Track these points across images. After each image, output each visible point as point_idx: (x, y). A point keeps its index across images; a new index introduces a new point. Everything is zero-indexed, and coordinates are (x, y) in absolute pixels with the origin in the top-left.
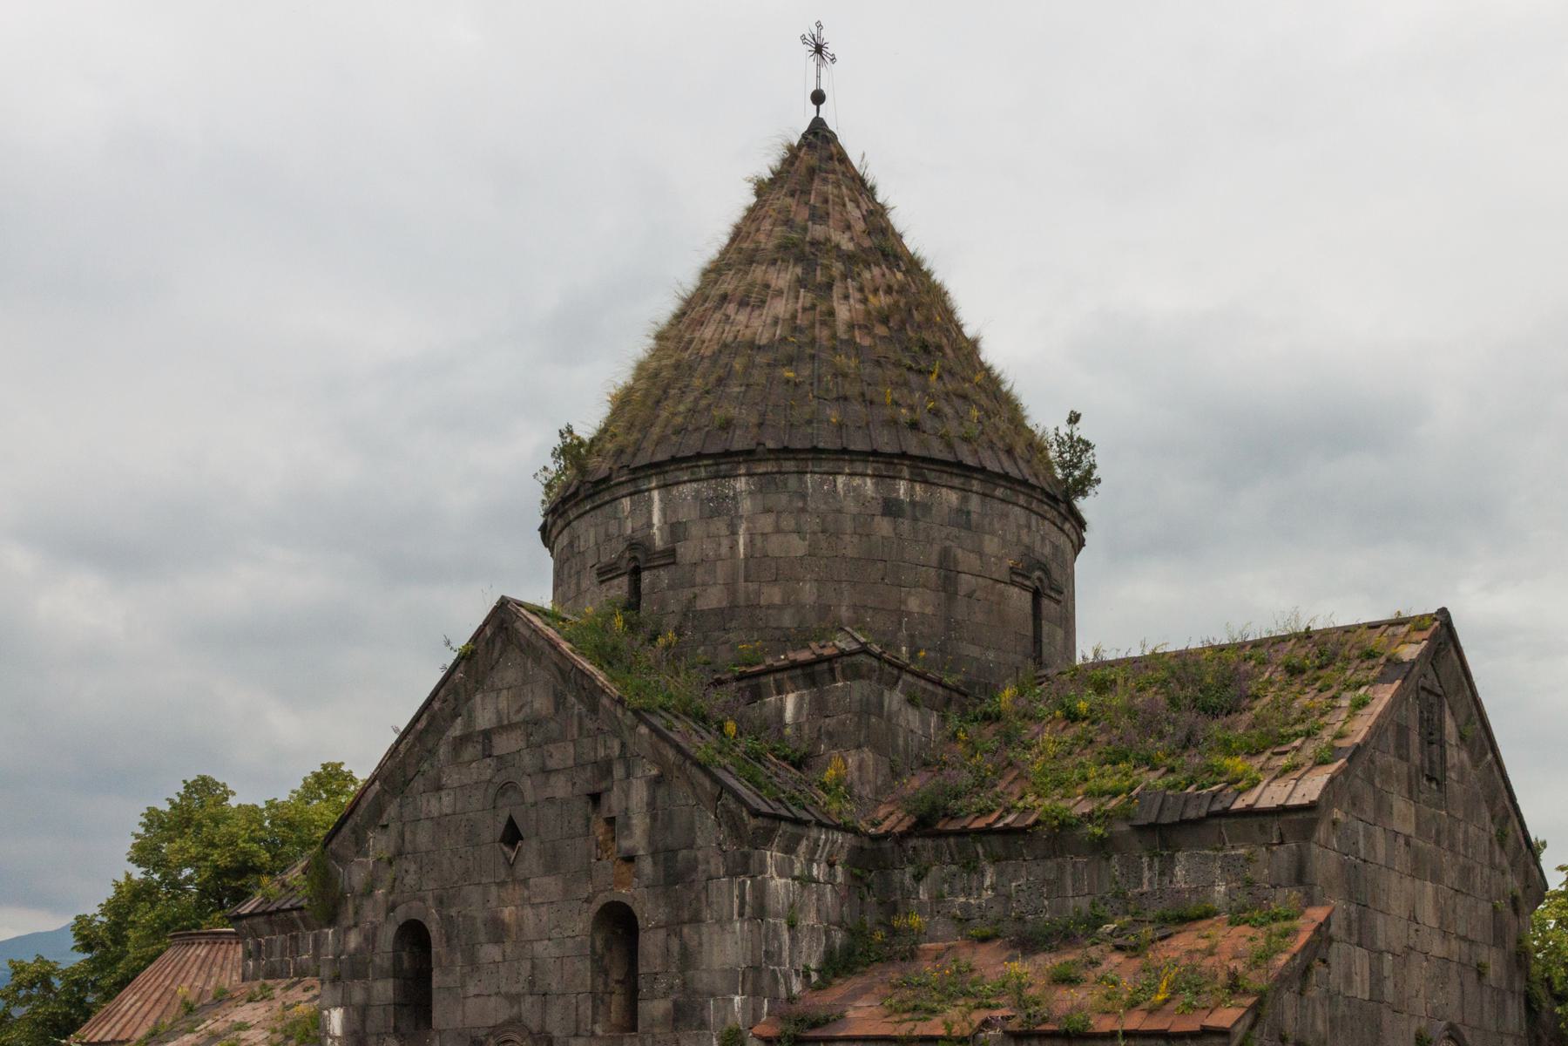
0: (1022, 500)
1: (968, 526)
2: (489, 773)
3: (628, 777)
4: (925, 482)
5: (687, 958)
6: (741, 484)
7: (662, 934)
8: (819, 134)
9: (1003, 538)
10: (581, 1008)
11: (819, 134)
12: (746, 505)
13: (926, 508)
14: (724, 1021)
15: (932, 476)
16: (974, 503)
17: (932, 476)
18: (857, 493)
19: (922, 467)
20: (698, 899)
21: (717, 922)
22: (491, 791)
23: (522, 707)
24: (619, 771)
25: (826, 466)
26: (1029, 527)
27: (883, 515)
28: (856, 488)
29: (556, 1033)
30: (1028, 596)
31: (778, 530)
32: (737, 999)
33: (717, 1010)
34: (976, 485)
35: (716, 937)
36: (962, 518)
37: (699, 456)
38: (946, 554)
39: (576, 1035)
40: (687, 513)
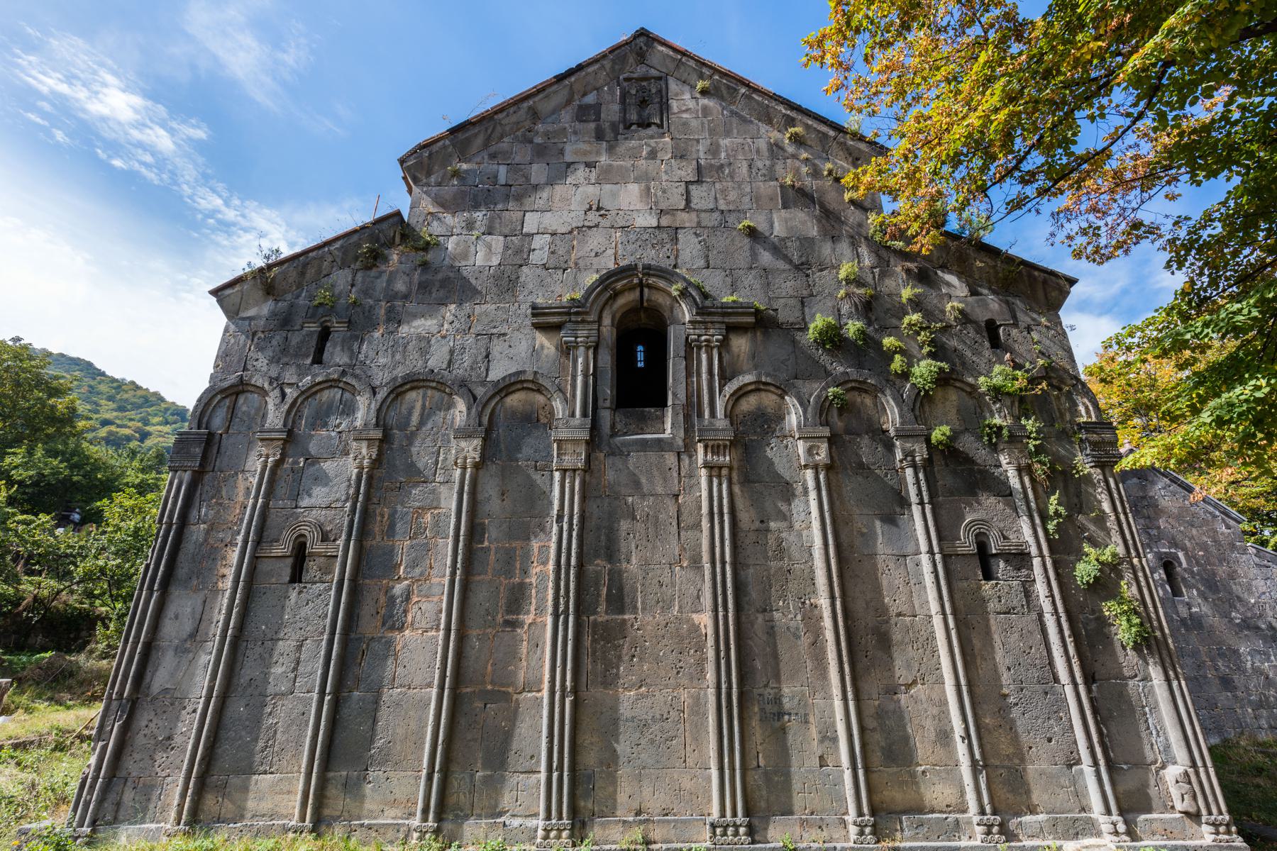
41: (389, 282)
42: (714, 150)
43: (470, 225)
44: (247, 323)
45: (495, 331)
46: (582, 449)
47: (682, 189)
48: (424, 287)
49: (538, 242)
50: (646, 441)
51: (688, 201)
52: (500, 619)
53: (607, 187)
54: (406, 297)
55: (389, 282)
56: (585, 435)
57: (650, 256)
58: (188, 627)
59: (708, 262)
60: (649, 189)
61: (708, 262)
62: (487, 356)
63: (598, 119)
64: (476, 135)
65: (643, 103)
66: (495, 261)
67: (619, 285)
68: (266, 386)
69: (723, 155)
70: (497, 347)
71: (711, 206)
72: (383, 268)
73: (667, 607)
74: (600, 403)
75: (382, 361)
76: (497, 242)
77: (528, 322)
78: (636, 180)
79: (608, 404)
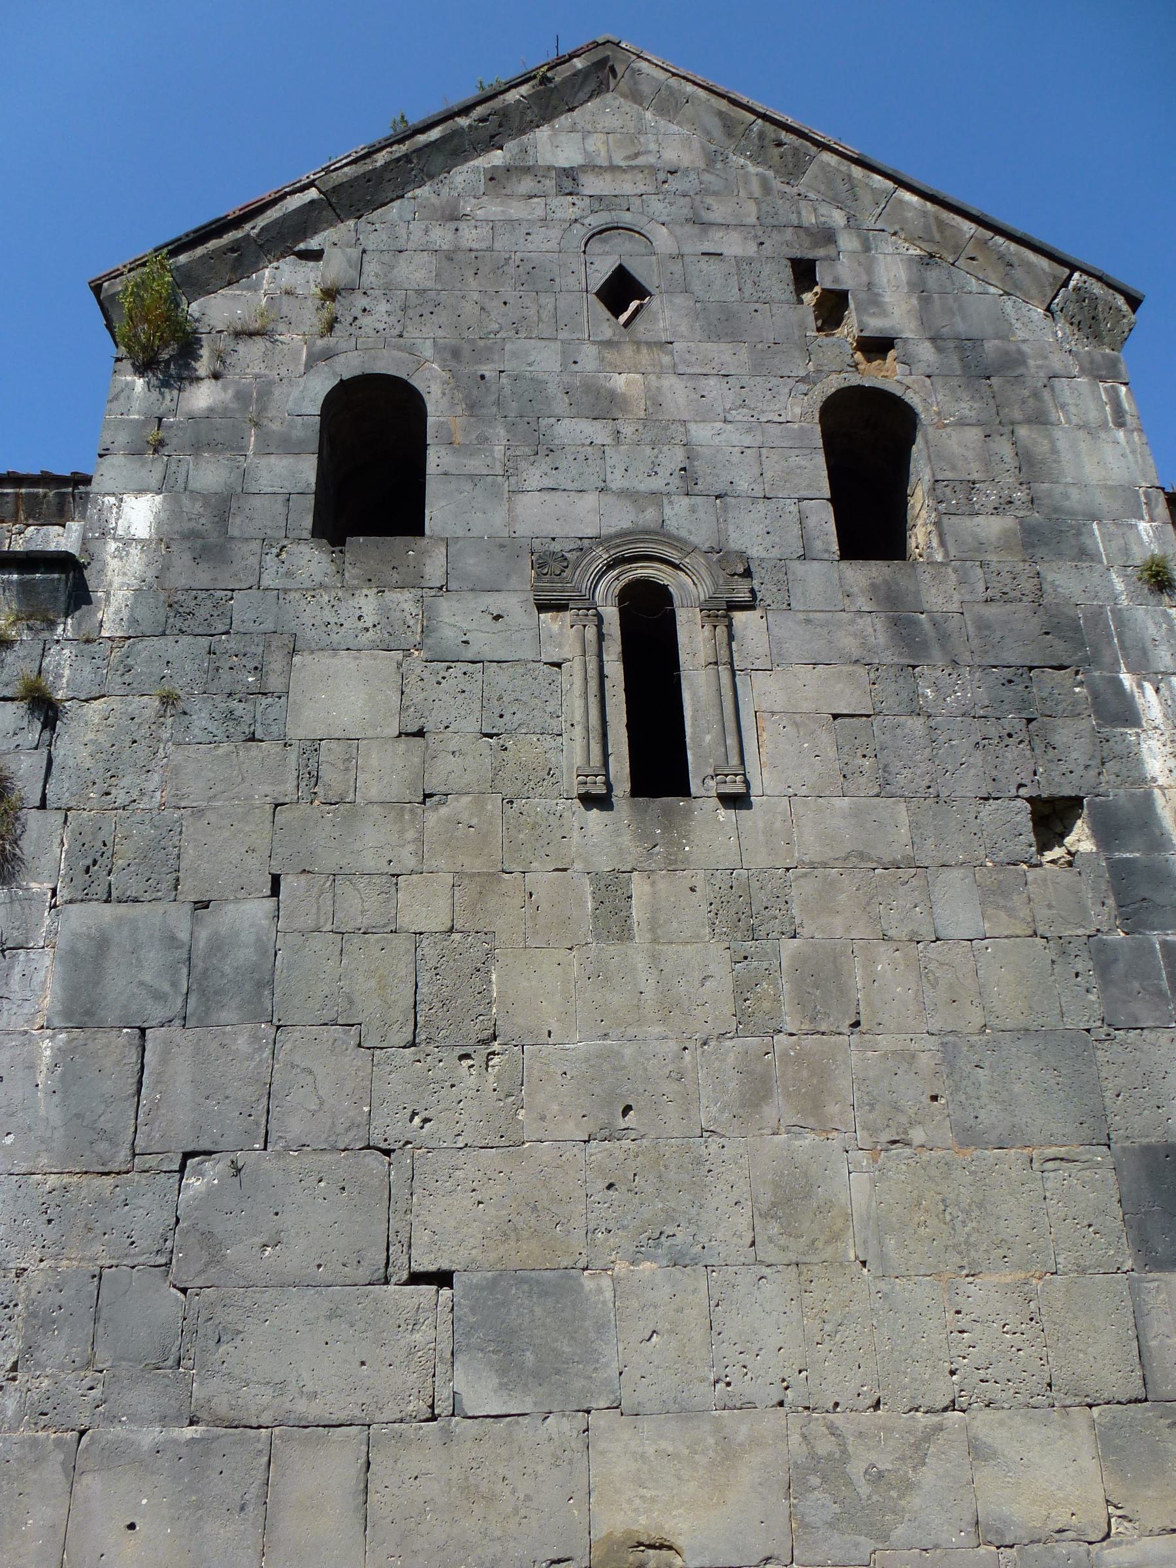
2: (572, 212)
3: (867, 249)
5: (1029, 467)
7: (973, 435)
10: (812, 522)
14: (1126, 551)
20: (1036, 395)
21: (1080, 427)
22: (579, 231)
23: (637, 155)
24: (847, 242)
29: (755, 552)
32: (1143, 526)
33: (1108, 538)
35: (1083, 446)
39: (803, 557)
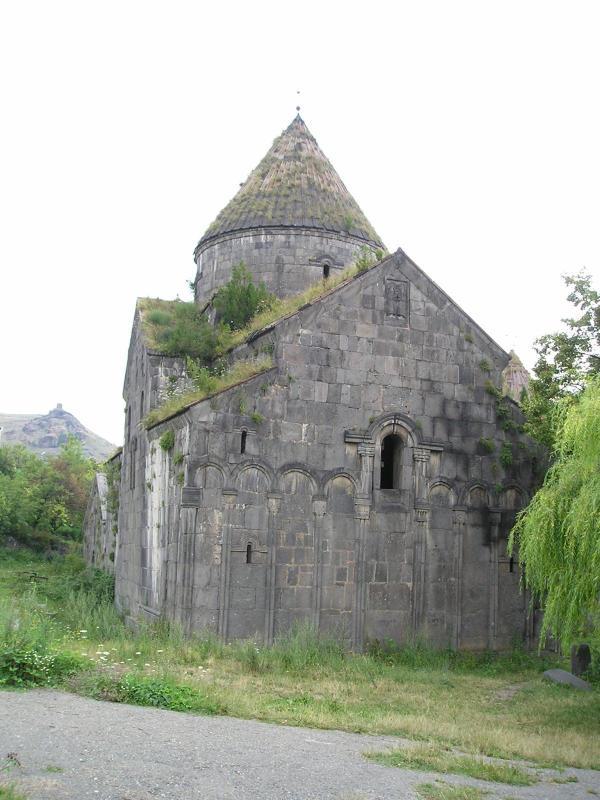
0: (317, 234)
1: (289, 247)
4: (271, 234)
6: (216, 247)
8: (298, 120)
9: (306, 250)
11: (298, 120)
12: (217, 254)
13: (271, 243)
15: (274, 232)
16: (292, 238)
17: (274, 232)
18: (248, 243)
19: (269, 228)
25: (239, 235)
26: (322, 243)
27: (256, 248)
28: (247, 240)
30: (322, 269)
31: (224, 260)
34: (293, 232)
36: (287, 245)
37: (206, 240)
38: (278, 258)
40: (206, 259)
41: (273, 406)
42: (430, 340)
43: (310, 375)
44: (203, 425)
45: (327, 442)
46: (368, 509)
47: (414, 365)
48: (289, 411)
49: (346, 388)
50: (393, 507)
51: (417, 373)
52: (335, 582)
53: (378, 357)
54: (282, 417)
55: (273, 406)
56: (368, 502)
57: (398, 405)
58: (206, 581)
59: (423, 410)
60: (398, 362)
61: (423, 410)
62: (324, 457)
63: (373, 308)
64: (312, 312)
65: (397, 299)
66: (324, 401)
67: (386, 424)
68: (221, 464)
69: (435, 344)
70: (329, 452)
71: (427, 377)
72: (268, 397)
73: (398, 578)
74: (375, 487)
75: (275, 455)
76: (324, 387)
77: (341, 438)
78: (393, 355)
79: (378, 485)
